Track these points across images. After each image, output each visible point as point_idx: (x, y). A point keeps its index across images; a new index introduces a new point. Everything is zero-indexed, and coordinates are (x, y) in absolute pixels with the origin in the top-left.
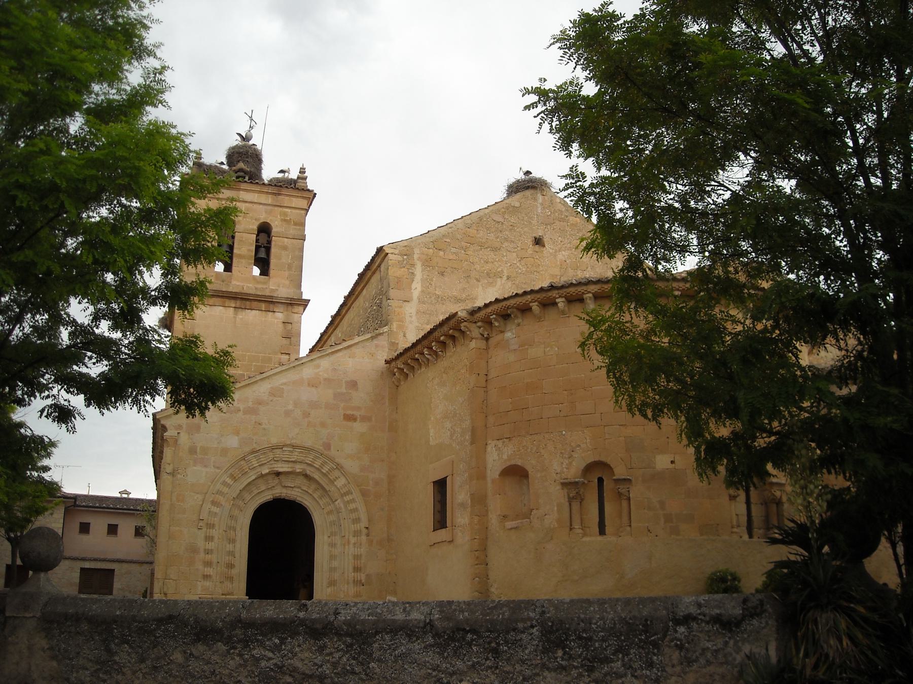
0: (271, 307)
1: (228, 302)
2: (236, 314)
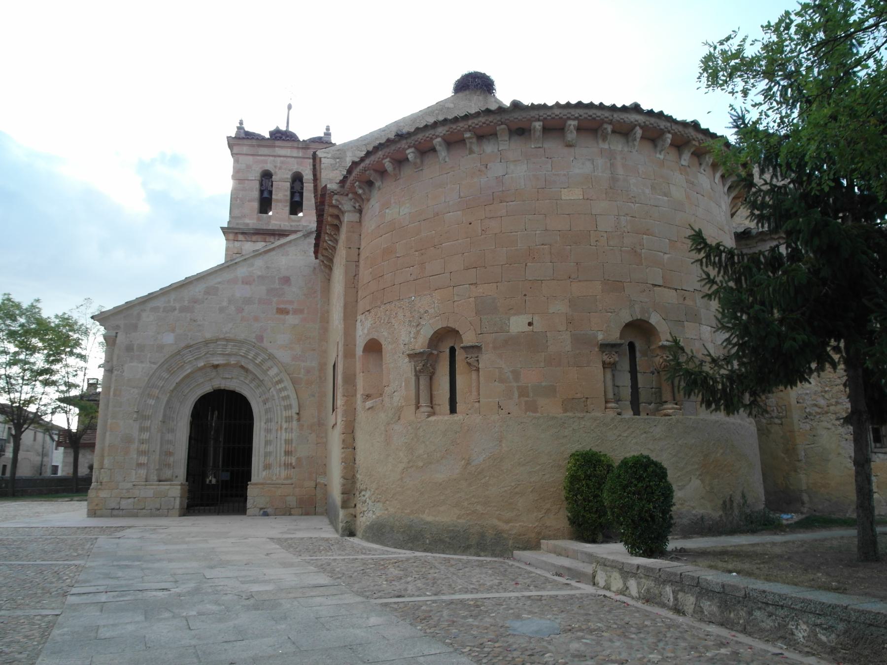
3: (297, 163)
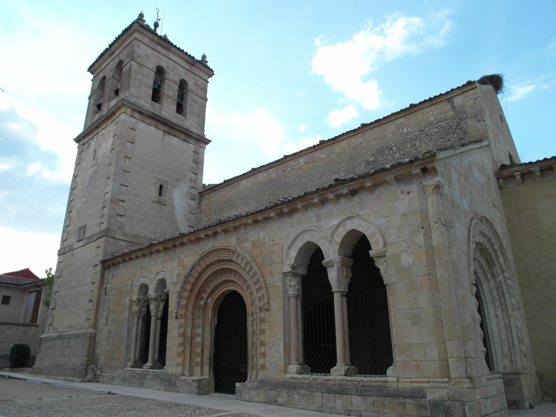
0: (187, 139)
1: (160, 126)
2: (164, 136)
3: (185, 73)
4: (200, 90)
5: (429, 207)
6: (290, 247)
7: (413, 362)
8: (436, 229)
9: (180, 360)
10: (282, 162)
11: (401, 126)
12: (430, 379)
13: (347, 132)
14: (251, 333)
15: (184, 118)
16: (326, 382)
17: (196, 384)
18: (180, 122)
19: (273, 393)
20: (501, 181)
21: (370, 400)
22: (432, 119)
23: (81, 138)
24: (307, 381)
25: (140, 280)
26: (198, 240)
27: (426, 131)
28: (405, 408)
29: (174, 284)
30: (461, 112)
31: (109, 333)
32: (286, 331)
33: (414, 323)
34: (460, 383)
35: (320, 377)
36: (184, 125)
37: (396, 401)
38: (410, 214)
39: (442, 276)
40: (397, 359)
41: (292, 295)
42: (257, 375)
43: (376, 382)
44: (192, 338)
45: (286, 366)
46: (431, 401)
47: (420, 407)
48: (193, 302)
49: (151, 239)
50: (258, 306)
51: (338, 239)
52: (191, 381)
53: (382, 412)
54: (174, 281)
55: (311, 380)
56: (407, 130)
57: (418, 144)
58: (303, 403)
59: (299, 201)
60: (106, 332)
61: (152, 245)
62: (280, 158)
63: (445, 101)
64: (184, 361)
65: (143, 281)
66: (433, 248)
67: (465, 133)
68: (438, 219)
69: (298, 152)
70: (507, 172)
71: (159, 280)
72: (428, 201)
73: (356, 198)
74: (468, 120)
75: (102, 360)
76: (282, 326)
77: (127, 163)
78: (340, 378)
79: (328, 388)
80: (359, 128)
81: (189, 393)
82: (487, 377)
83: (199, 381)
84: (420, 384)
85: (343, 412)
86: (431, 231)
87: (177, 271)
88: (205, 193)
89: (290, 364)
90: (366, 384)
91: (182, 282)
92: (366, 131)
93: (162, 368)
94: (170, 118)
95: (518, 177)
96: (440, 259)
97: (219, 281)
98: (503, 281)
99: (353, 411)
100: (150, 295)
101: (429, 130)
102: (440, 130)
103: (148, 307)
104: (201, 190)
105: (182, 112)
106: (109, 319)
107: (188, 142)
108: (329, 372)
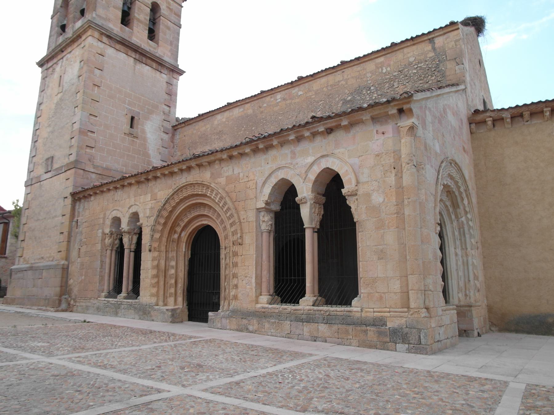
1: (130, 52)
2: (135, 64)
4: (173, 15)
5: (402, 148)
6: (264, 183)
7: (377, 294)
8: (408, 170)
9: (154, 290)
10: (258, 97)
11: (380, 65)
12: (391, 309)
13: (326, 69)
14: (224, 266)
15: (156, 45)
16: (295, 311)
17: (170, 313)
18: (152, 49)
19: (245, 321)
20: (473, 126)
21: (335, 327)
22: (412, 59)
23: (45, 62)
24: (277, 311)
25: (112, 213)
26: (172, 174)
27: (405, 72)
28: (367, 334)
29: (147, 217)
30: (441, 54)
31: (82, 264)
32: (258, 264)
33: (379, 259)
34: (418, 312)
35: (289, 307)
36: (157, 53)
37: (359, 328)
38: (384, 154)
39: (409, 215)
40: (362, 291)
41: (265, 231)
42: (229, 305)
43: (341, 311)
44: (166, 271)
45: (257, 297)
46: (391, 329)
47: (380, 333)
48: (167, 235)
49: (122, 172)
50: (232, 240)
51: (312, 177)
52: (165, 310)
53: (345, 338)
54: (148, 215)
55: (281, 309)
56: (387, 70)
57: (396, 85)
58: (272, 331)
59: (275, 138)
60: (79, 264)
61: (124, 178)
62: (257, 94)
63: (426, 42)
64: (158, 292)
65: (115, 214)
66: (403, 187)
67: (443, 76)
68: (410, 160)
69: (275, 88)
70: (479, 117)
71: (132, 213)
72: (402, 143)
73: (331, 137)
74: (447, 62)
75: (75, 291)
76: (255, 259)
77: (96, 92)
78: (308, 307)
79: (296, 317)
80: (338, 65)
81: (164, 322)
82: (442, 308)
83: (173, 310)
84: (382, 314)
85: (310, 338)
86: (402, 172)
87: (150, 205)
88: (179, 127)
89: (261, 295)
90: (332, 313)
91: (155, 215)
92: (345, 68)
93: (136, 298)
94: (141, 45)
95: (490, 123)
96: (409, 198)
97: (193, 216)
98: (465, 222)
99: (319, 338)
100: (123, 229)
101: (408, 71)
102: (419, 71)
103: (121, 240)
104: (175, 123)
105: (154, 38)
106: (82, 251)
107: (161, 72)
108: (298, 303)
